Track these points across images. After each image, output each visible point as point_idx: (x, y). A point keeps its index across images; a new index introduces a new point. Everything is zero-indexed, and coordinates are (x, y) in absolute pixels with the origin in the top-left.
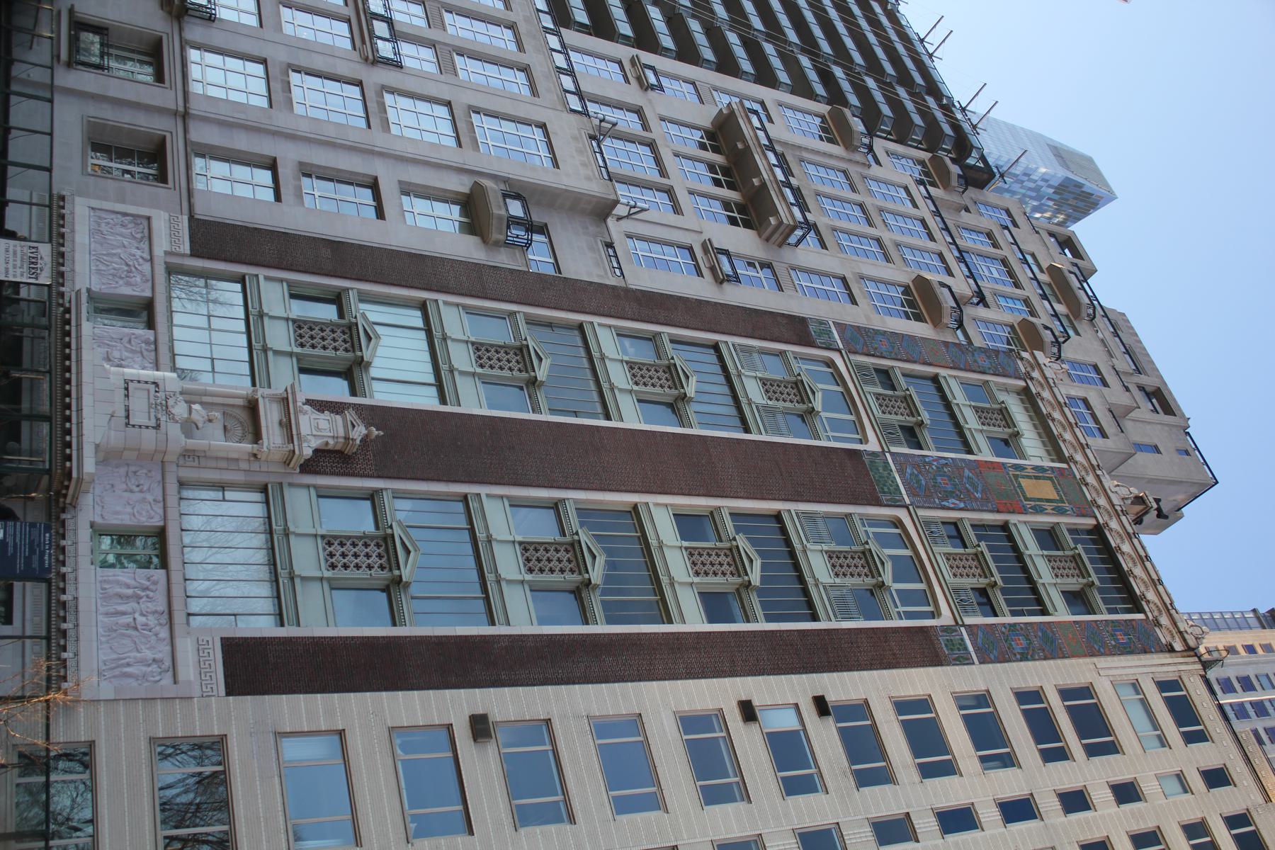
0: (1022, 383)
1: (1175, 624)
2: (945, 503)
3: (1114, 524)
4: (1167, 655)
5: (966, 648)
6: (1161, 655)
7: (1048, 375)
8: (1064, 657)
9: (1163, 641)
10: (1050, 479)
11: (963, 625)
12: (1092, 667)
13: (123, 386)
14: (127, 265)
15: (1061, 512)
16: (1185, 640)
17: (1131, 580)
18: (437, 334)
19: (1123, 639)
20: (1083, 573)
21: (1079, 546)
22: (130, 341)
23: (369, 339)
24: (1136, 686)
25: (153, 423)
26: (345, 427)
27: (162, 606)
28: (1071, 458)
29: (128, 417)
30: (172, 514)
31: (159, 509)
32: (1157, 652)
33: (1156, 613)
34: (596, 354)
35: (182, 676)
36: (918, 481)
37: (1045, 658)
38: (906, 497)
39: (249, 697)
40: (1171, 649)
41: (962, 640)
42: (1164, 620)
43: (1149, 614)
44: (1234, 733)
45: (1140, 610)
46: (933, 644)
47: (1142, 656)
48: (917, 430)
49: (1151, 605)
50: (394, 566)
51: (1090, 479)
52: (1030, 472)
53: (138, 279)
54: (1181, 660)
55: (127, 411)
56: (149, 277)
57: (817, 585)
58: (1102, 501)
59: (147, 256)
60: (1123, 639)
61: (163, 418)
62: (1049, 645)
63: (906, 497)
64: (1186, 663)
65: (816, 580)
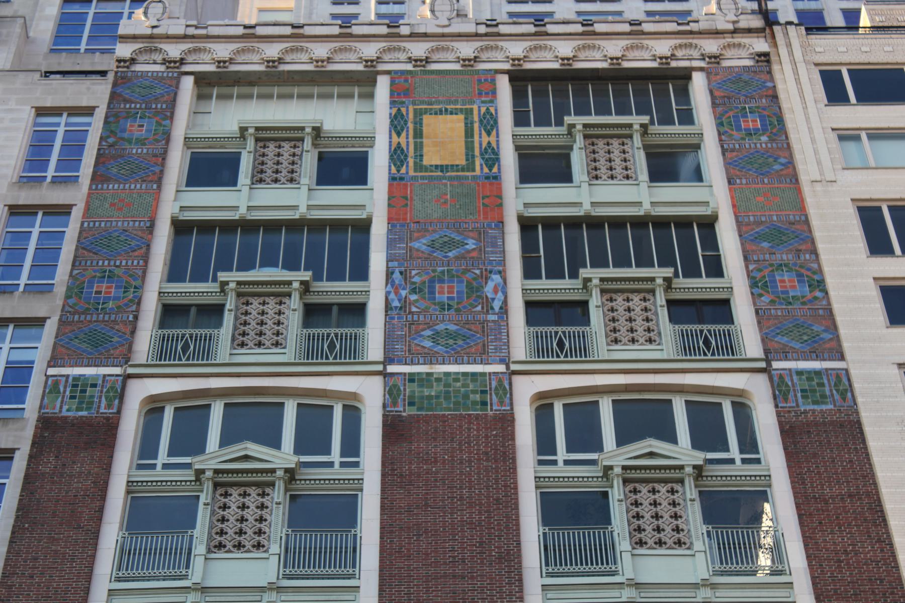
0: (188, 83)
1: (717, 33)
2: (497, 305)
3: (517, 49)
4: (775, 68)
5: (818, 373)
6: (777, 76)
7: (180, 30)
8: (807, 222)
9: (749, 63)
10: (419, 114)
11: (768, 361)
12: (818, 187)
15: (490, 123)
16: (749, 31)
17: (626, 65)
19: (752, 122)
20: (623, 134)
21: (568, 120)
24: (847, 136)
28: (370, 63)
32: (772, 79)
33: (696, 54)
36: (449, 334)
37: (814, 252)
38: (488, 369)
40: (764, 57)
41: (800, 373)
42: (711, 46)
43: (696, 64)
45: (685, 76)
46: (817, 424)
47: (785, 105)
48: (313, 299)
49: (679, 53)
51: (419, 49)
52: (406, 140)
54: (783, 51)
57: (714, 586)
58: (467, 49)
60: (752, 122)
62: (783, 242)
63: (488, 369)
64: (789, 45)
65: (705, 584)
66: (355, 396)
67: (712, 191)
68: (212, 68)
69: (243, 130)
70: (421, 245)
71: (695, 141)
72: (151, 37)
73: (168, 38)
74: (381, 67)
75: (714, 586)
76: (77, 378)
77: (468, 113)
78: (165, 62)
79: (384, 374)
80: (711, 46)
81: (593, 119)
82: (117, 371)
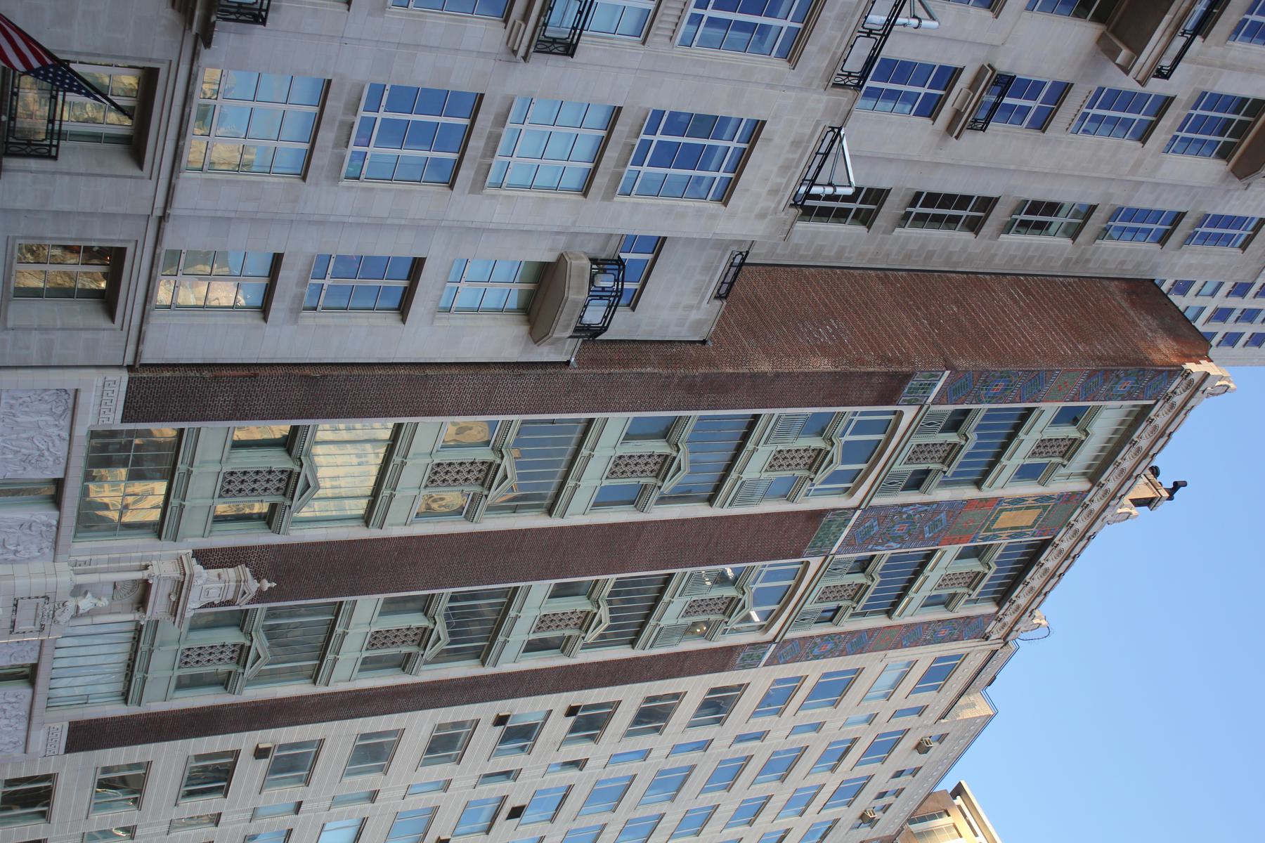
1: (1016, 622)
13: (12, 602)
14: (38, 449)
18: (397, 459)
22: (30, 527)
23: (308, 486)
25: (38, 627)
26: (236, 592)
27: (24, 712)
29: (13, 627)
30: (45, 659)
31: (35, 654)
34: (585, 452)
35: (31, 749)
39: (82, 753)
44: (981, 670)
45: (1000, 603)
50: (242, 662)
53: (51, 463)
55: (14, 622)
56: (63, 462)
57: (655, 627)
59: (65, 434)
61: (47, 623)
66: (852, 494)
67: (912, 612)
68: (1152, 415)
69: (1087, 434)
70: (943, 516)
71: (950, 607)
72: (1197, 389)
73: (1192, 396)
74: (1095, 489)
75: (655, 627)
76: (935, 385)
77: (1031, 527)
78: (1174, 392)
79: (856, 509)
80: (1009, 619)
81: (987, 577)
82: (930, 400)
